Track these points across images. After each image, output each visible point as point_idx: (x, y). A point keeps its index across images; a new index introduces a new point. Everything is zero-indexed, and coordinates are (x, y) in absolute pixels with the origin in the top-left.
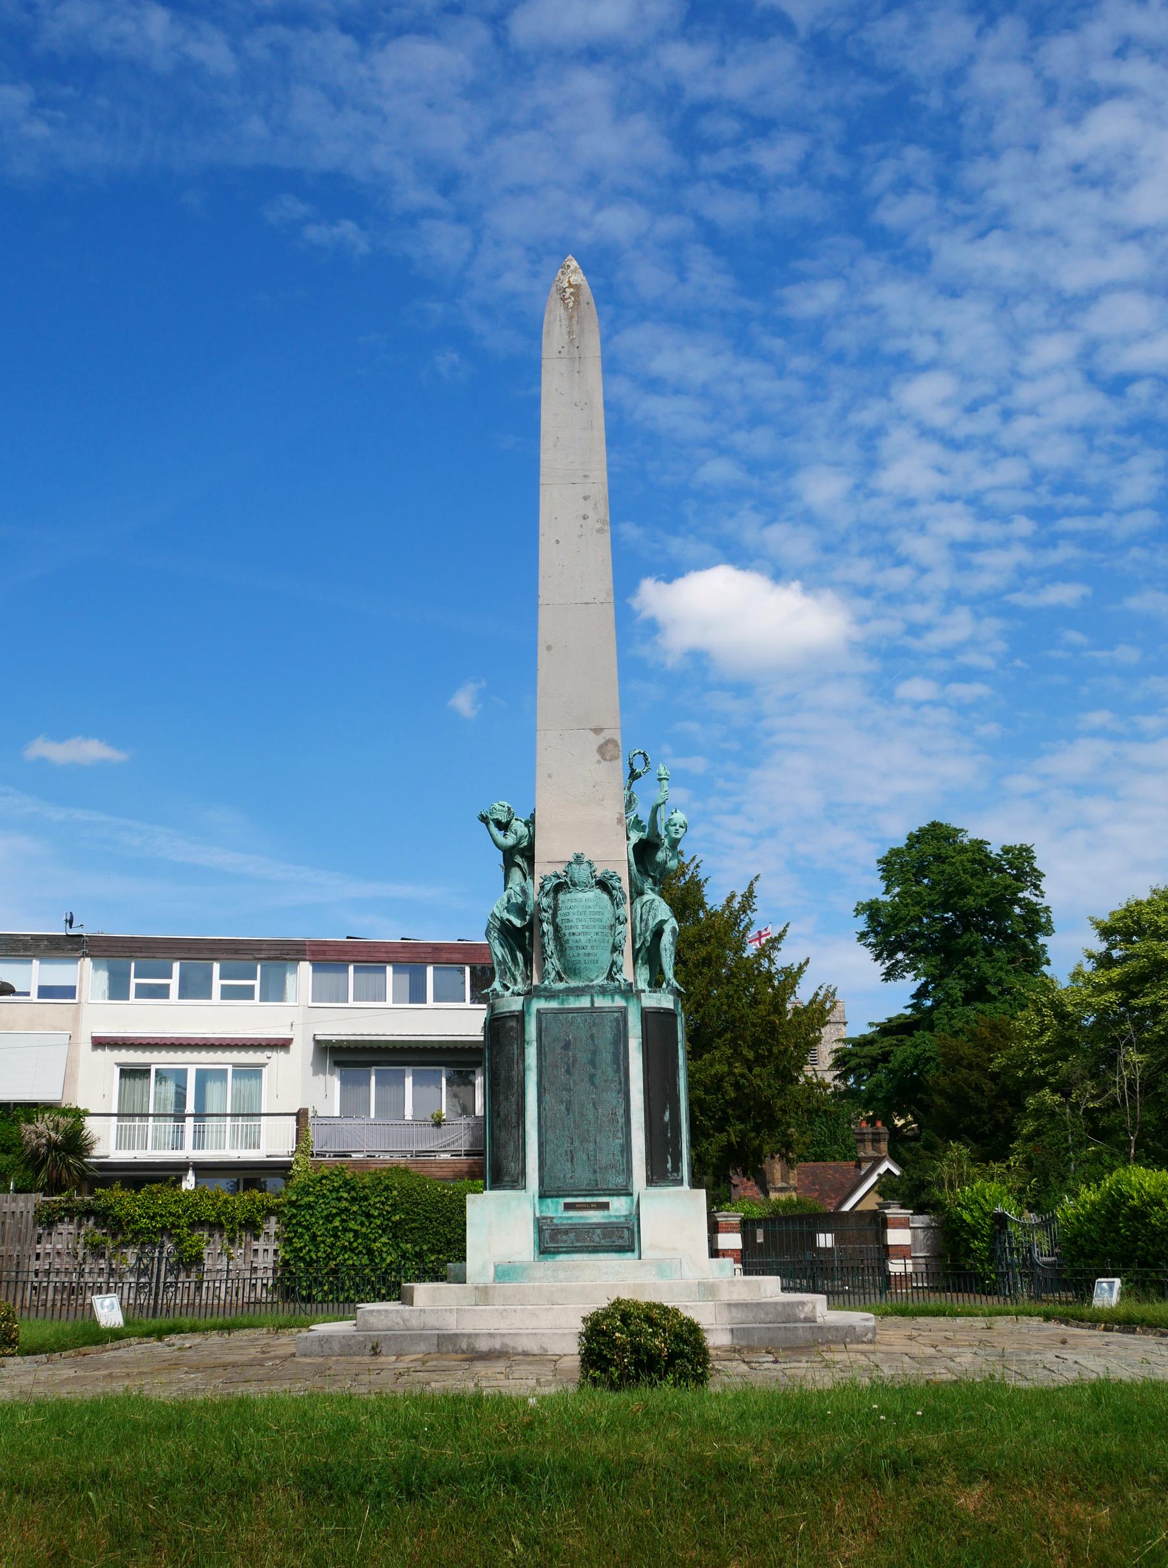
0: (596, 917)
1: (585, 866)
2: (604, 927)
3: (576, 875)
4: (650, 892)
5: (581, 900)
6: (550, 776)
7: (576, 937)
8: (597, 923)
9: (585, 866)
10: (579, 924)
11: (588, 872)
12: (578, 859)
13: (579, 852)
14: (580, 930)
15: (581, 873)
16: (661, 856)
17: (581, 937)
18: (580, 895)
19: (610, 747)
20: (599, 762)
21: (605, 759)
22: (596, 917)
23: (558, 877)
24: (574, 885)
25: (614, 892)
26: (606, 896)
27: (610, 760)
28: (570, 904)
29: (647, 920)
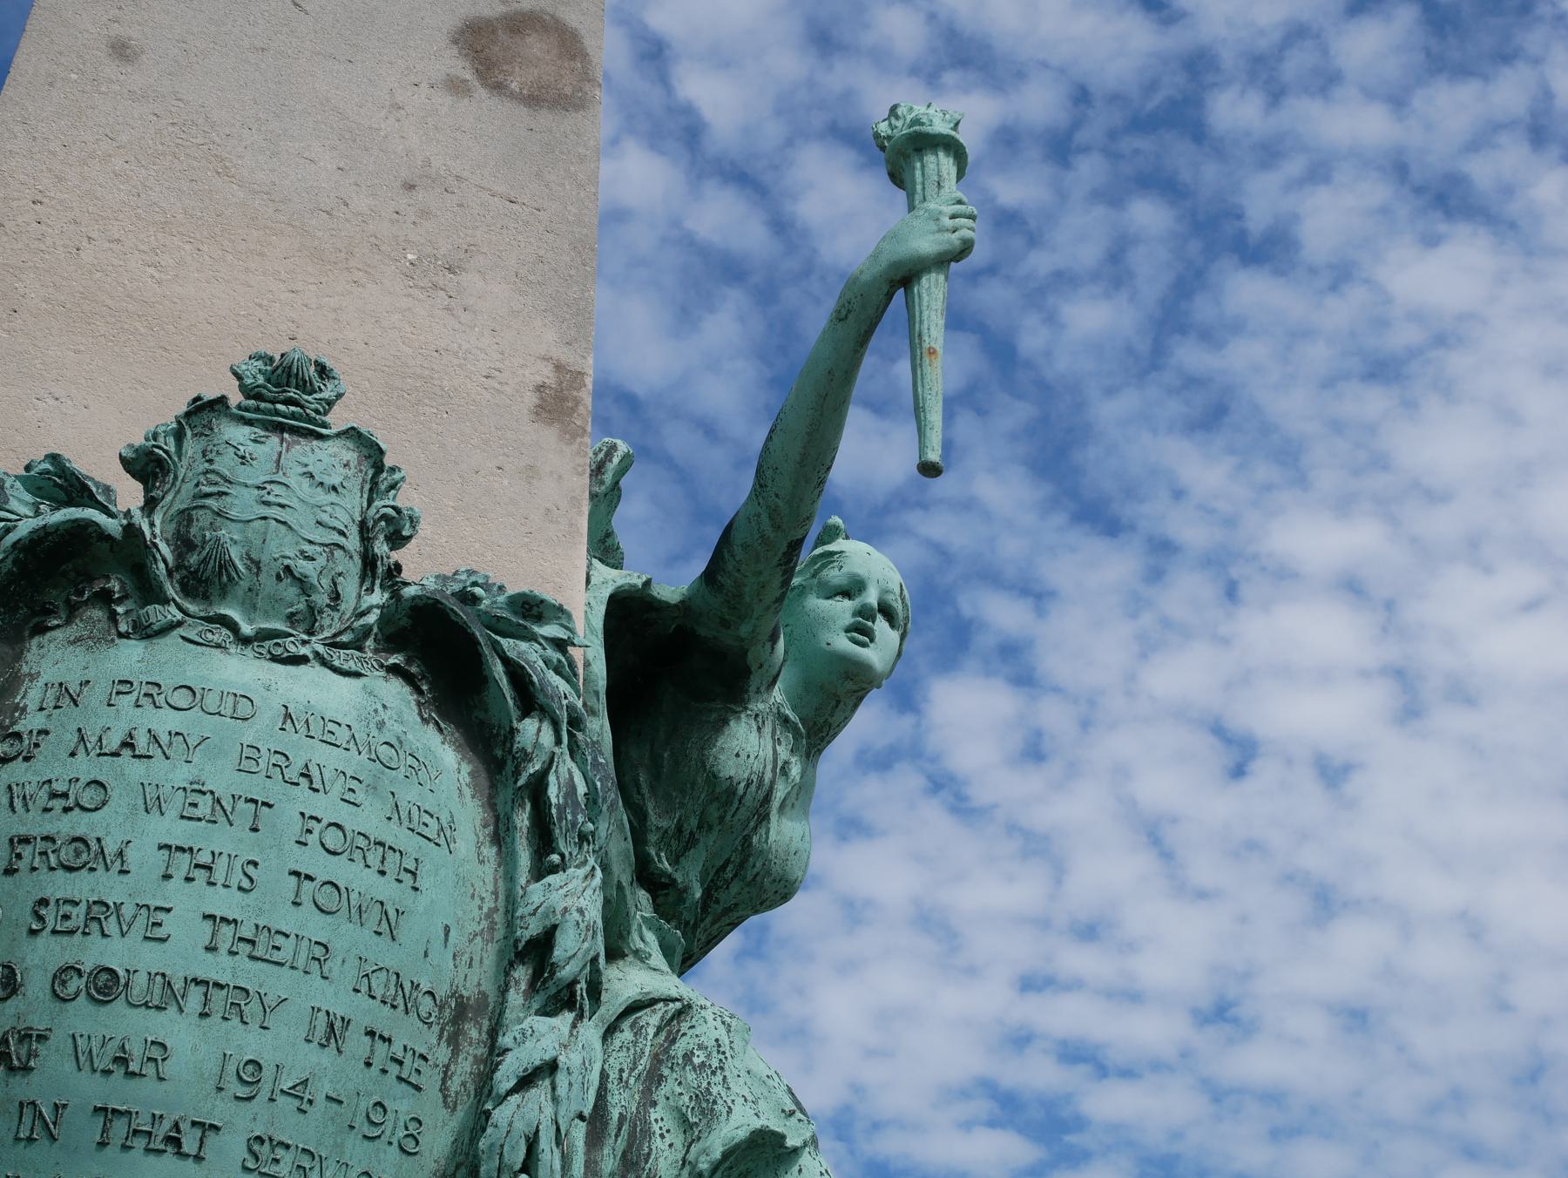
0: (358, 877)
1: (333, 459)
2: (402, 996)
3: (242, 503)
4: (658, 959)
5: (240, 706)
6: (122, 50)
7: (126, 1024)
8: (348, 937)
9: (333, 459)
10: (187, 903)
11: (349, 507)
12: (285, 396)
13: (309, 342)
14: (185, 951)
15: (288, 500)
16: (747, 745)
17: (180, 1031)
18: (239, 670)
19: (535, 46)
20: (456, 87)
21: (498, 88)
22: (358, 877)
23: (61, 483)
24: (205, 578)
25: (532, 732)
26: (446, 760)
27: (533, 100)
28: (127, 717)
29: (639, 1132)
